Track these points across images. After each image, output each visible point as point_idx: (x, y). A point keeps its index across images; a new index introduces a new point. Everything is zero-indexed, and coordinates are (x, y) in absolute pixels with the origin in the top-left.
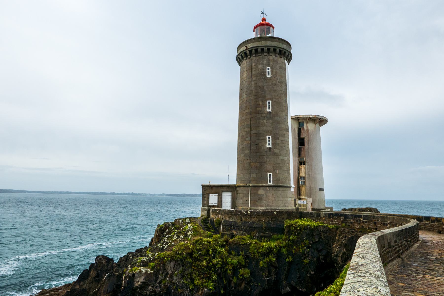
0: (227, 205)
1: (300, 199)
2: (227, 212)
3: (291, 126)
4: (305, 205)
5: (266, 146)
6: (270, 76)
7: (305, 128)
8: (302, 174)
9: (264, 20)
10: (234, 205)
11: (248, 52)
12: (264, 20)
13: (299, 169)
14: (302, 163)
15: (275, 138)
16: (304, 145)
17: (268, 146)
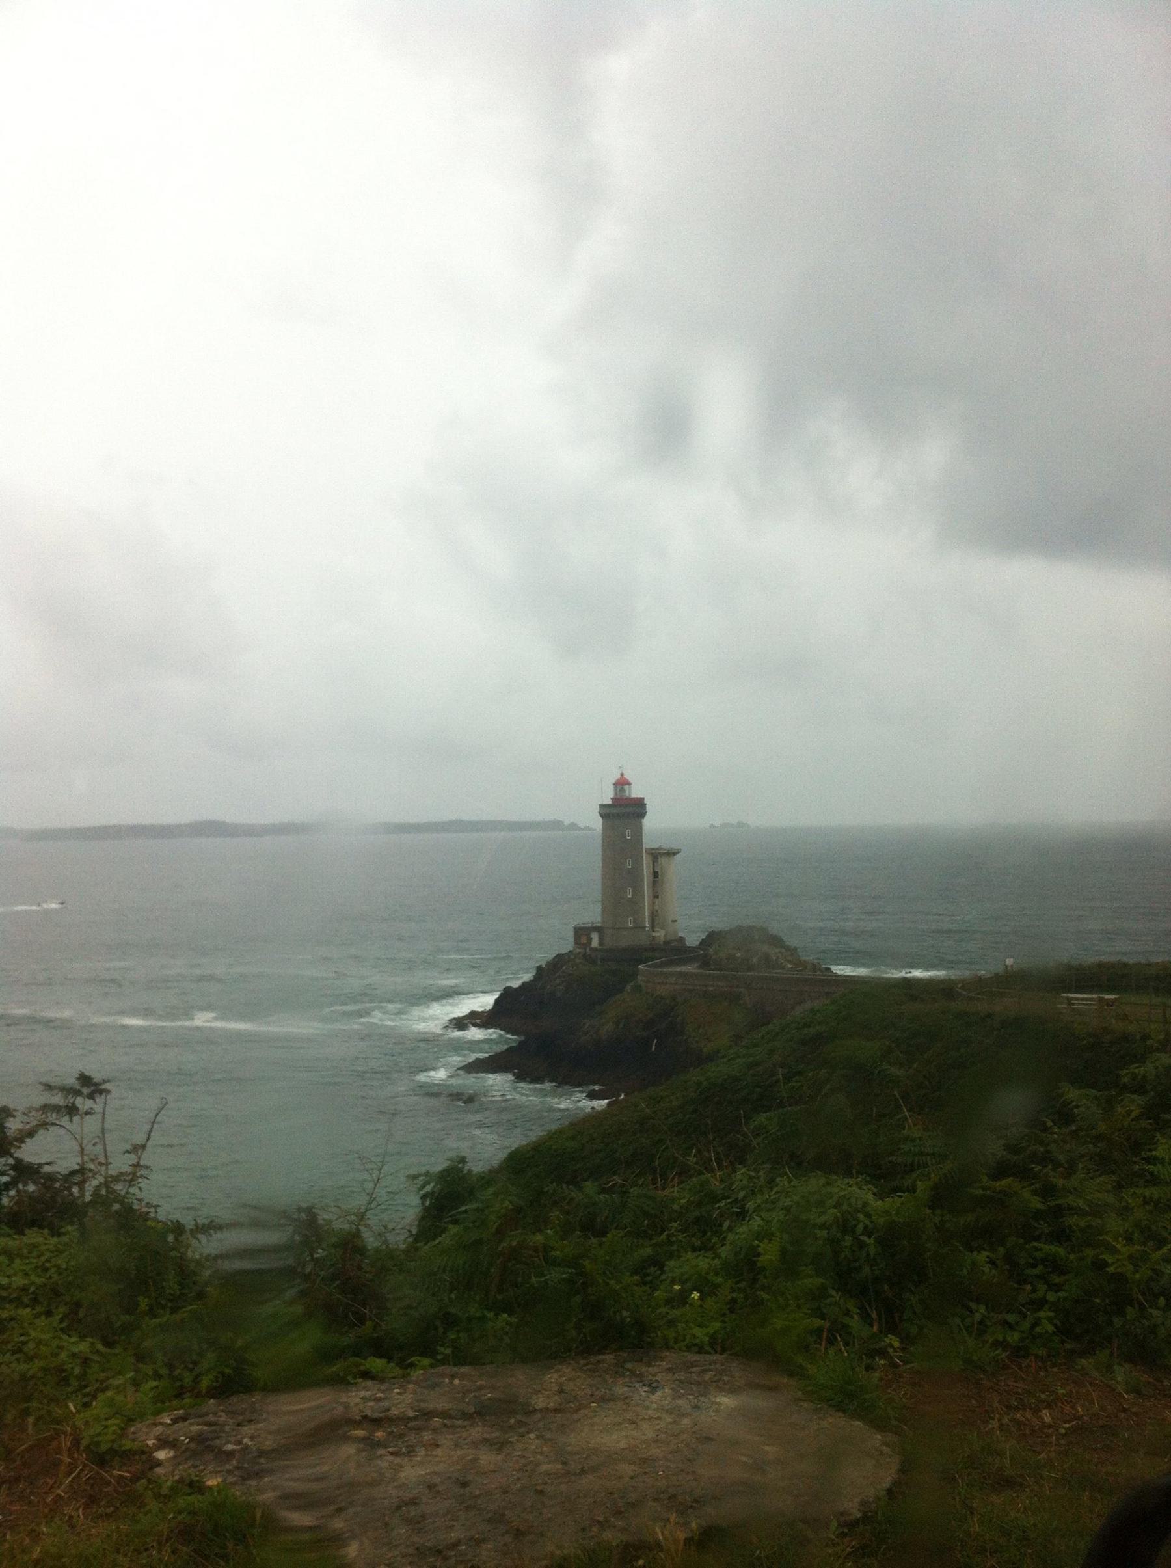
0: (595, 943)
1: (653, 931)
2: (595, 950)
3: (646, 860)
4: (659, 936)
5: (627, 896)
6: (629, 838)
7: (660, 862)
8: (656, 907)
9: (622, 775)
10: (601, 943)
11: (611, 815)
12: (622, 775)
13: (654, 903)
14: (656, 896)
15: (634, 889)
16: (658, 877)
17: (629, 896)
